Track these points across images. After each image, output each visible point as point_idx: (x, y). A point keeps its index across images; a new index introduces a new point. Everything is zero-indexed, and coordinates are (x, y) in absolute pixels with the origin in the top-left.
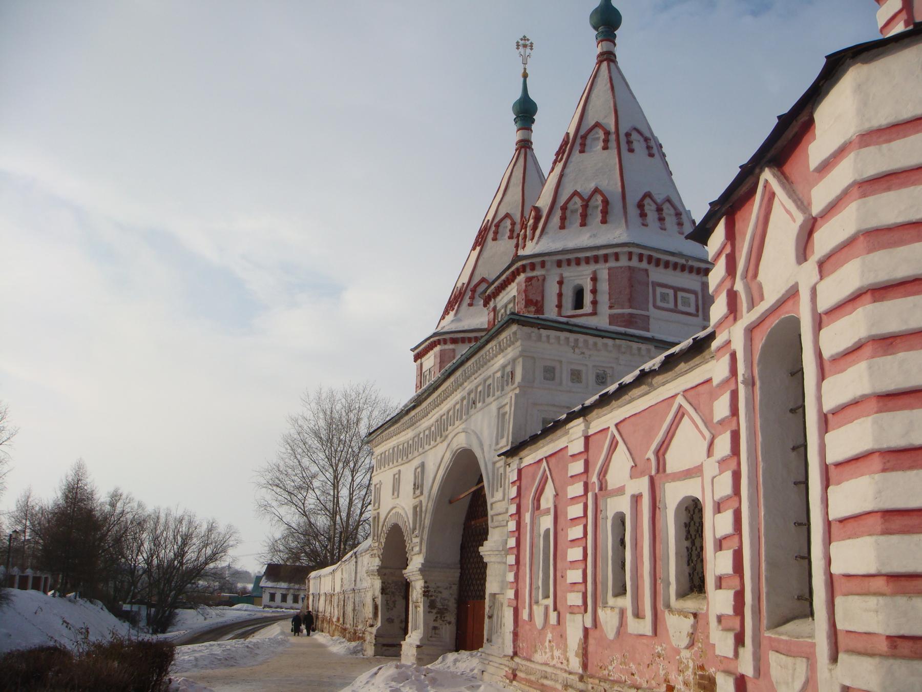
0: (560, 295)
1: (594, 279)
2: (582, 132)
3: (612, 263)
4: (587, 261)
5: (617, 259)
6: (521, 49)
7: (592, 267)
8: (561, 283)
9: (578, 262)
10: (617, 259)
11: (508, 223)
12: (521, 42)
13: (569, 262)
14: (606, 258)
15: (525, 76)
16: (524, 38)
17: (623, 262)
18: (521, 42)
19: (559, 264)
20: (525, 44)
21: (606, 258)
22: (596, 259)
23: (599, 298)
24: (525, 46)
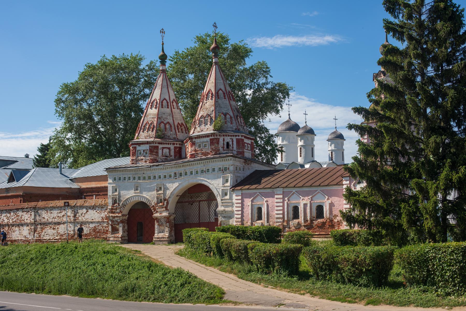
0: (224, 144)
1: (233, 141)
2: (217, 91)
3: (237, 137)
4: (231, 136)
5: (239, 136)
6: (162, 33)
7: (232, 137)
8: (224, 140)
9: (229, 136)
10: (239, 136)
11: (165, 102)
12: (162, 31)
13: (226, 136)
14: (236, 136)
15: (163, 44)
16: (163, 29)
17: (240, 137)
18: (162, 31)
19: (224, 135)
20: (162, 32)
21: (236, 136)
22: (233, 136)
23: (234, 146)
24: (163, 32)
